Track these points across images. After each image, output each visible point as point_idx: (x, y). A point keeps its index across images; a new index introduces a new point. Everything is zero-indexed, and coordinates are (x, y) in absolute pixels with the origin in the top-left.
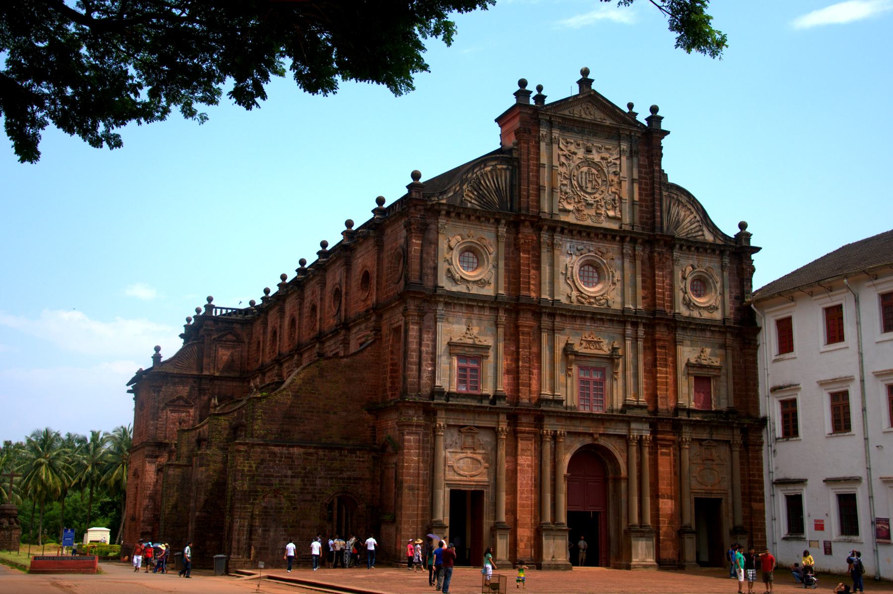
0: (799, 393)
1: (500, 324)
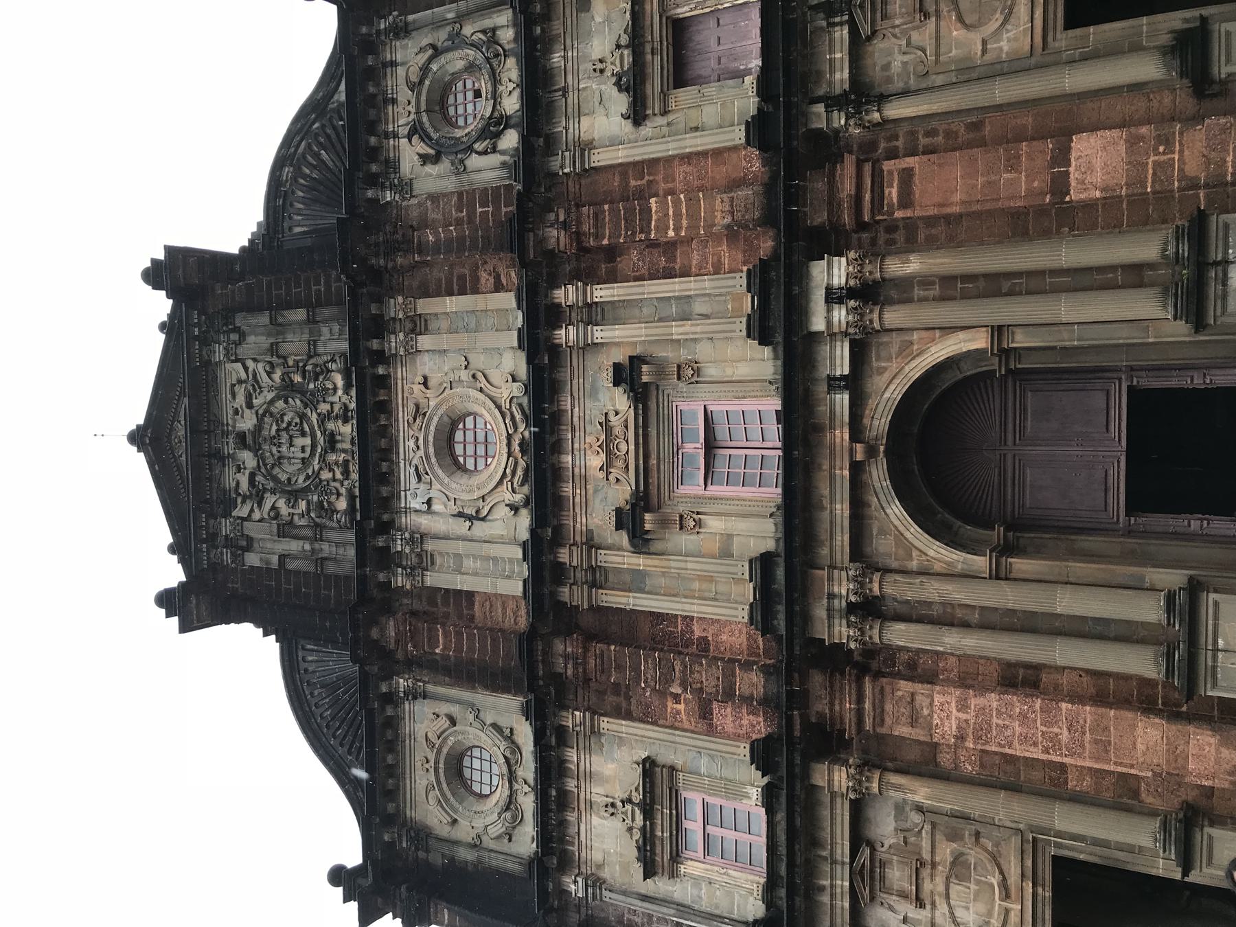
1: (592, 726)
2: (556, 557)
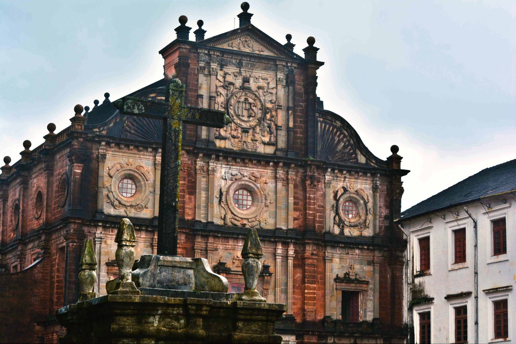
0: (432, 307)
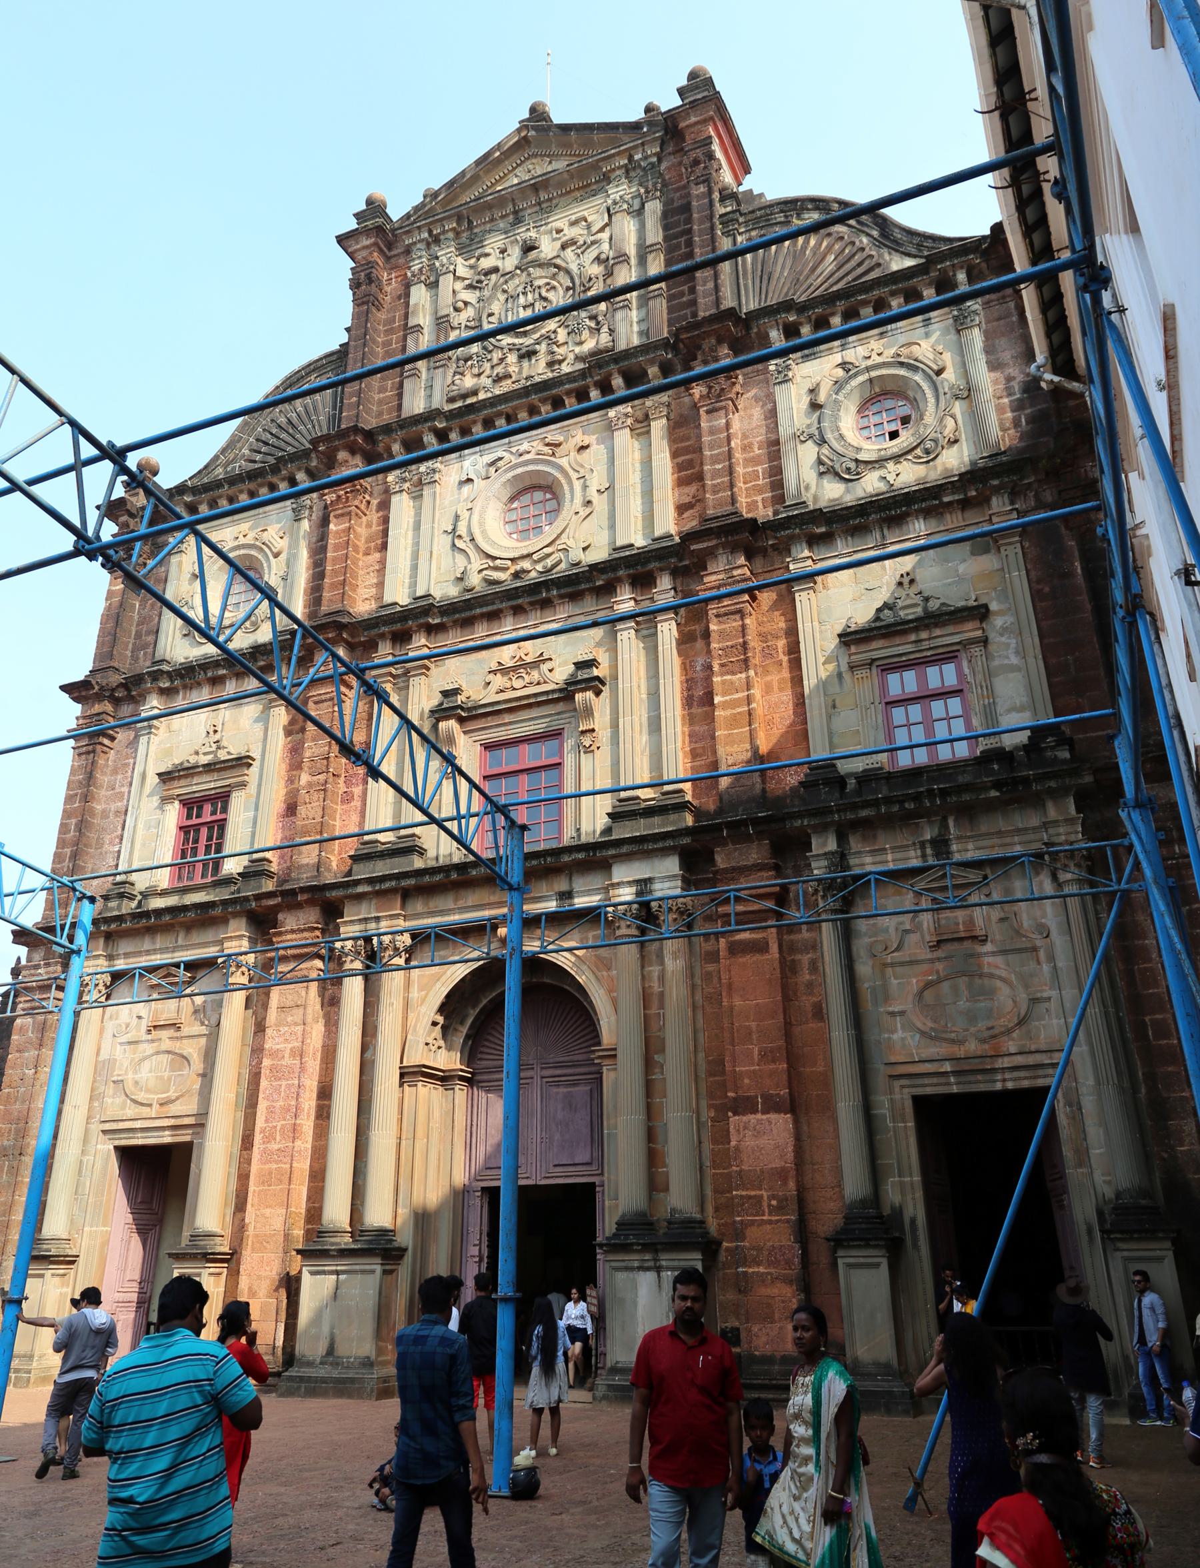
2: (416, 632)
